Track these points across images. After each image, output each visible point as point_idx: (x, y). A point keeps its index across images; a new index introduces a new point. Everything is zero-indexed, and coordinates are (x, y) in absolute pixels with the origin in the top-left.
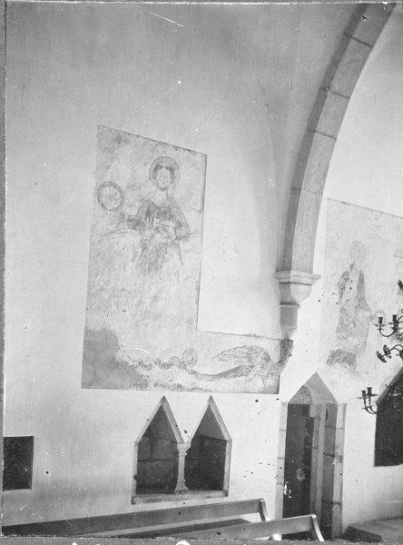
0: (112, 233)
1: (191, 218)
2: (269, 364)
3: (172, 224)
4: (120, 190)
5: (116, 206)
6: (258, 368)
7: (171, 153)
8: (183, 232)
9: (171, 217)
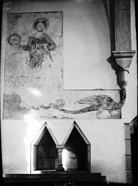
0: (15, 54)
1: (56, 41)
2: (112, 103)
3: (46, 45)
4: (19, 36)
5: (17, 43)
6: (105, 106)
7: (44, 15)
8: (52, 46)
9: (45, 42)
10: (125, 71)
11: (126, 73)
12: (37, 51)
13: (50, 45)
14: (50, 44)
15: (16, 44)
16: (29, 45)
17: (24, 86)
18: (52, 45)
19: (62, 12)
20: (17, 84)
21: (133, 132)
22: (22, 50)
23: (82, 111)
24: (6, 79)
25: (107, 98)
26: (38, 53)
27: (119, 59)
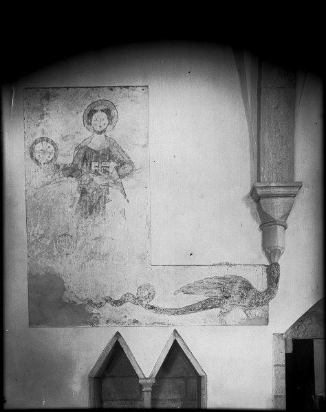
0: (48, 184)
3: (113, 165)
4: (53, 143)
6: (236, 298)
8: (128, 168)
9: (111, 158)
10: (278, 226)
11: (280, 229)
12: (95, 178)
13: (121, 166)
14: (122, 163)
15: (48, 163)
16: (77, 165)
17: (71, 257)
18: (126, 165)
19: (147, 86)
20: (55, 253)
21: (290, 350)
22: (61, 176)
23: (191, 309)
24: (31, 241)
25: (240, 281)
26: (96, 184)
27: (267, 200)
